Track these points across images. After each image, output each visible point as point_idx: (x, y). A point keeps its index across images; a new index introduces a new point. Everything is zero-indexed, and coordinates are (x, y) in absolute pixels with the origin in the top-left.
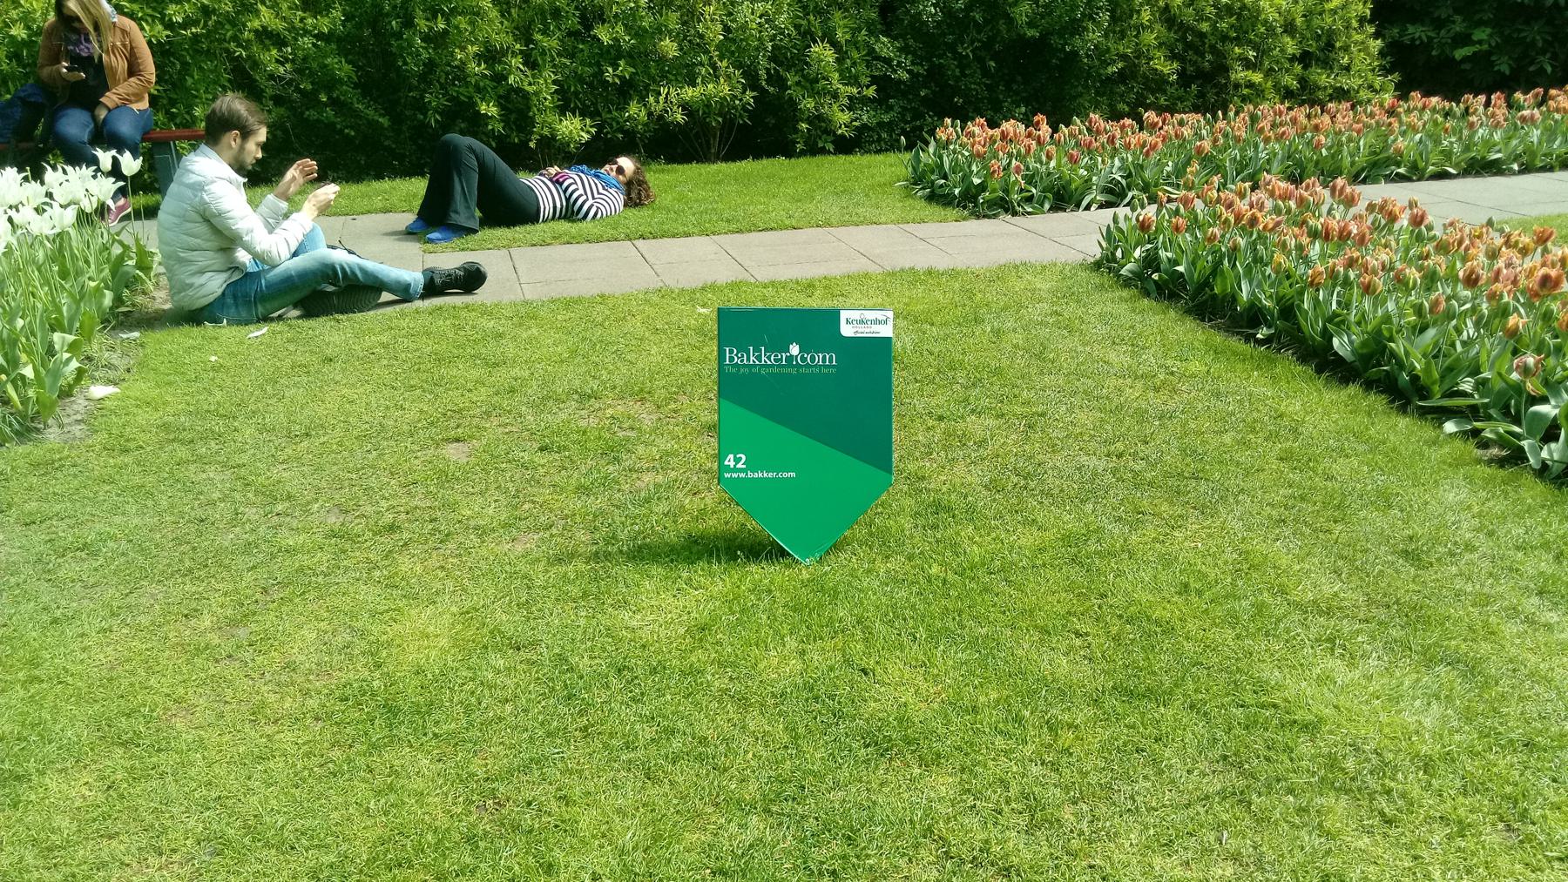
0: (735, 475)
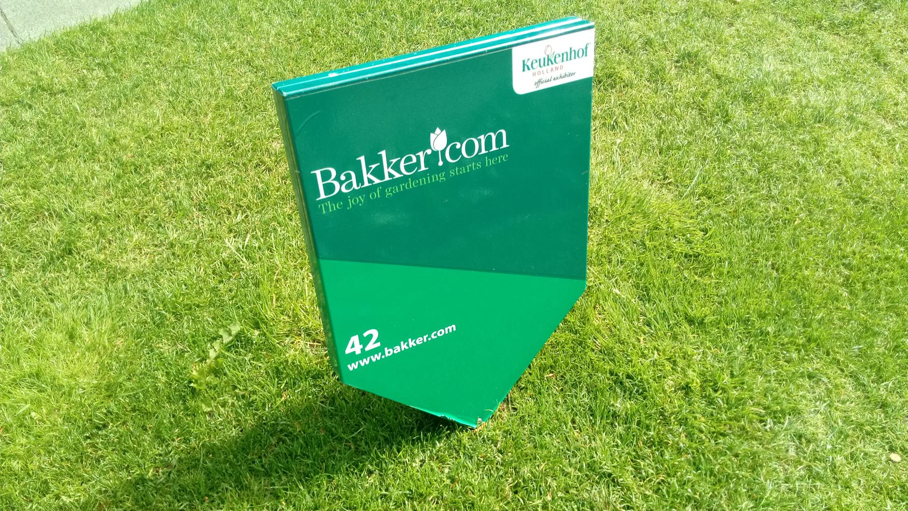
0: (366, 361)
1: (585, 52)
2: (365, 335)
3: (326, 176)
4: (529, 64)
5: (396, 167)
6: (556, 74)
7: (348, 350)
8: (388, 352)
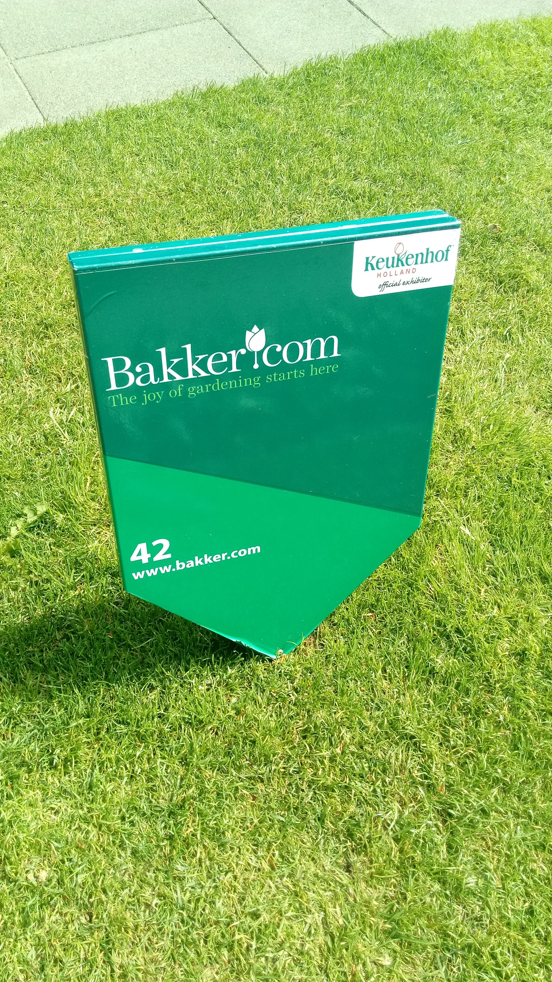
0: (153, 572)
1: (445, 255)
2: (155, 543)
3: (119, 365)
4: (374, 262)
5: (203, 365)
6: (407, 277)
7: (134, 558)
8: (179, 565)
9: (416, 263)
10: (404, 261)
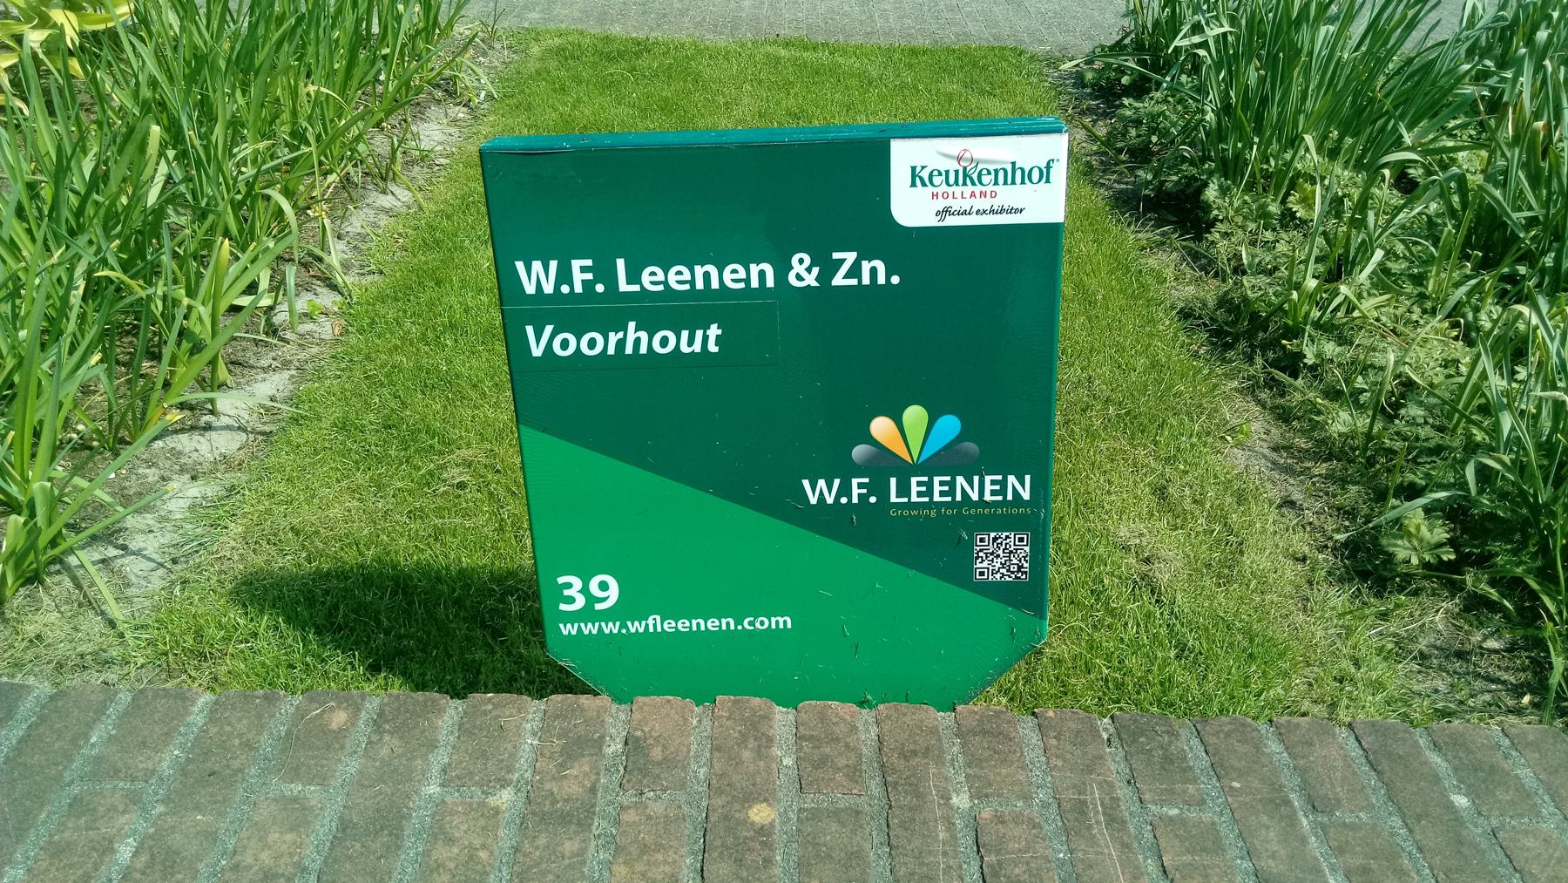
1: (1045, 174)
6: (984, 204)
9: (996, 183)
10: (975, 177)
